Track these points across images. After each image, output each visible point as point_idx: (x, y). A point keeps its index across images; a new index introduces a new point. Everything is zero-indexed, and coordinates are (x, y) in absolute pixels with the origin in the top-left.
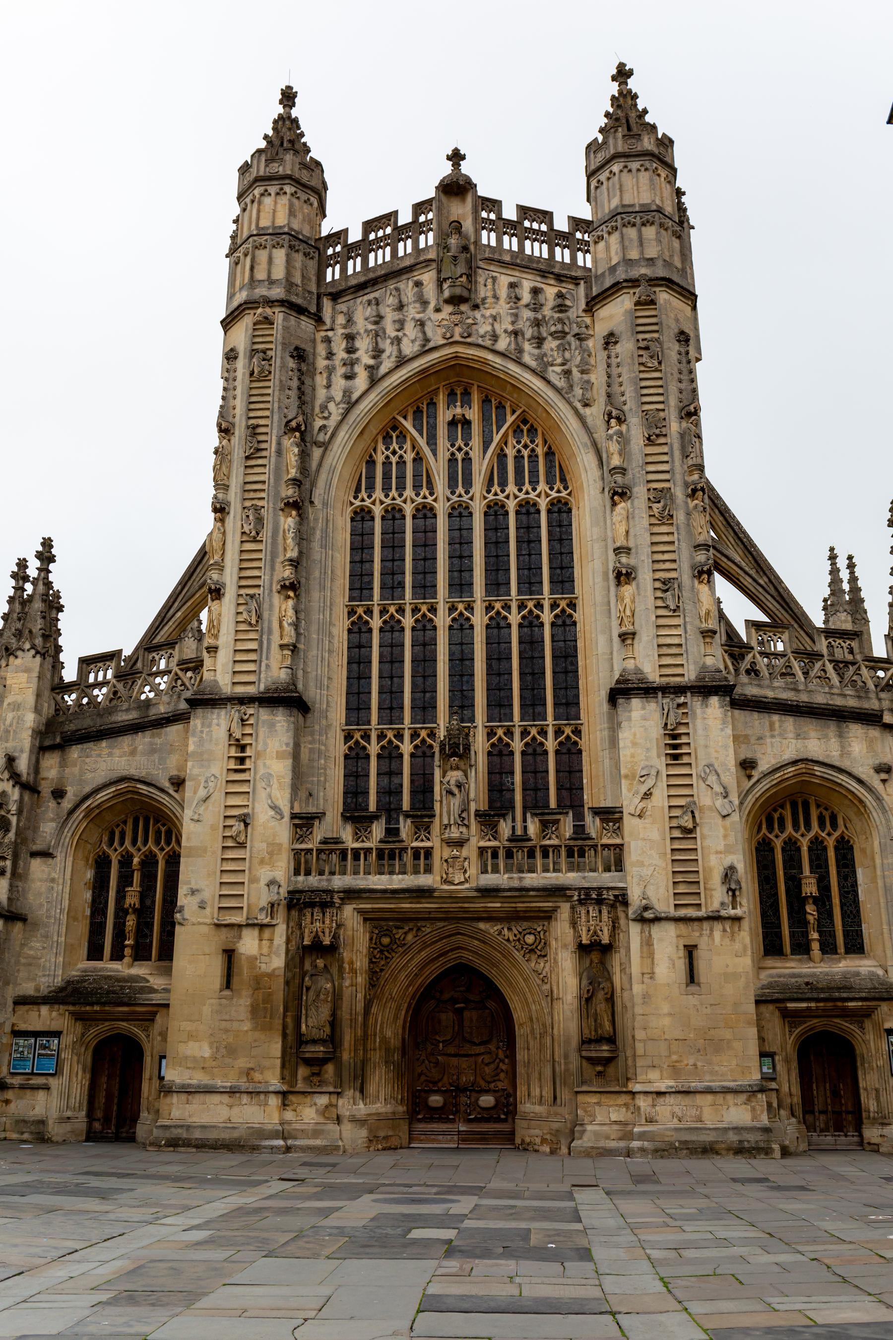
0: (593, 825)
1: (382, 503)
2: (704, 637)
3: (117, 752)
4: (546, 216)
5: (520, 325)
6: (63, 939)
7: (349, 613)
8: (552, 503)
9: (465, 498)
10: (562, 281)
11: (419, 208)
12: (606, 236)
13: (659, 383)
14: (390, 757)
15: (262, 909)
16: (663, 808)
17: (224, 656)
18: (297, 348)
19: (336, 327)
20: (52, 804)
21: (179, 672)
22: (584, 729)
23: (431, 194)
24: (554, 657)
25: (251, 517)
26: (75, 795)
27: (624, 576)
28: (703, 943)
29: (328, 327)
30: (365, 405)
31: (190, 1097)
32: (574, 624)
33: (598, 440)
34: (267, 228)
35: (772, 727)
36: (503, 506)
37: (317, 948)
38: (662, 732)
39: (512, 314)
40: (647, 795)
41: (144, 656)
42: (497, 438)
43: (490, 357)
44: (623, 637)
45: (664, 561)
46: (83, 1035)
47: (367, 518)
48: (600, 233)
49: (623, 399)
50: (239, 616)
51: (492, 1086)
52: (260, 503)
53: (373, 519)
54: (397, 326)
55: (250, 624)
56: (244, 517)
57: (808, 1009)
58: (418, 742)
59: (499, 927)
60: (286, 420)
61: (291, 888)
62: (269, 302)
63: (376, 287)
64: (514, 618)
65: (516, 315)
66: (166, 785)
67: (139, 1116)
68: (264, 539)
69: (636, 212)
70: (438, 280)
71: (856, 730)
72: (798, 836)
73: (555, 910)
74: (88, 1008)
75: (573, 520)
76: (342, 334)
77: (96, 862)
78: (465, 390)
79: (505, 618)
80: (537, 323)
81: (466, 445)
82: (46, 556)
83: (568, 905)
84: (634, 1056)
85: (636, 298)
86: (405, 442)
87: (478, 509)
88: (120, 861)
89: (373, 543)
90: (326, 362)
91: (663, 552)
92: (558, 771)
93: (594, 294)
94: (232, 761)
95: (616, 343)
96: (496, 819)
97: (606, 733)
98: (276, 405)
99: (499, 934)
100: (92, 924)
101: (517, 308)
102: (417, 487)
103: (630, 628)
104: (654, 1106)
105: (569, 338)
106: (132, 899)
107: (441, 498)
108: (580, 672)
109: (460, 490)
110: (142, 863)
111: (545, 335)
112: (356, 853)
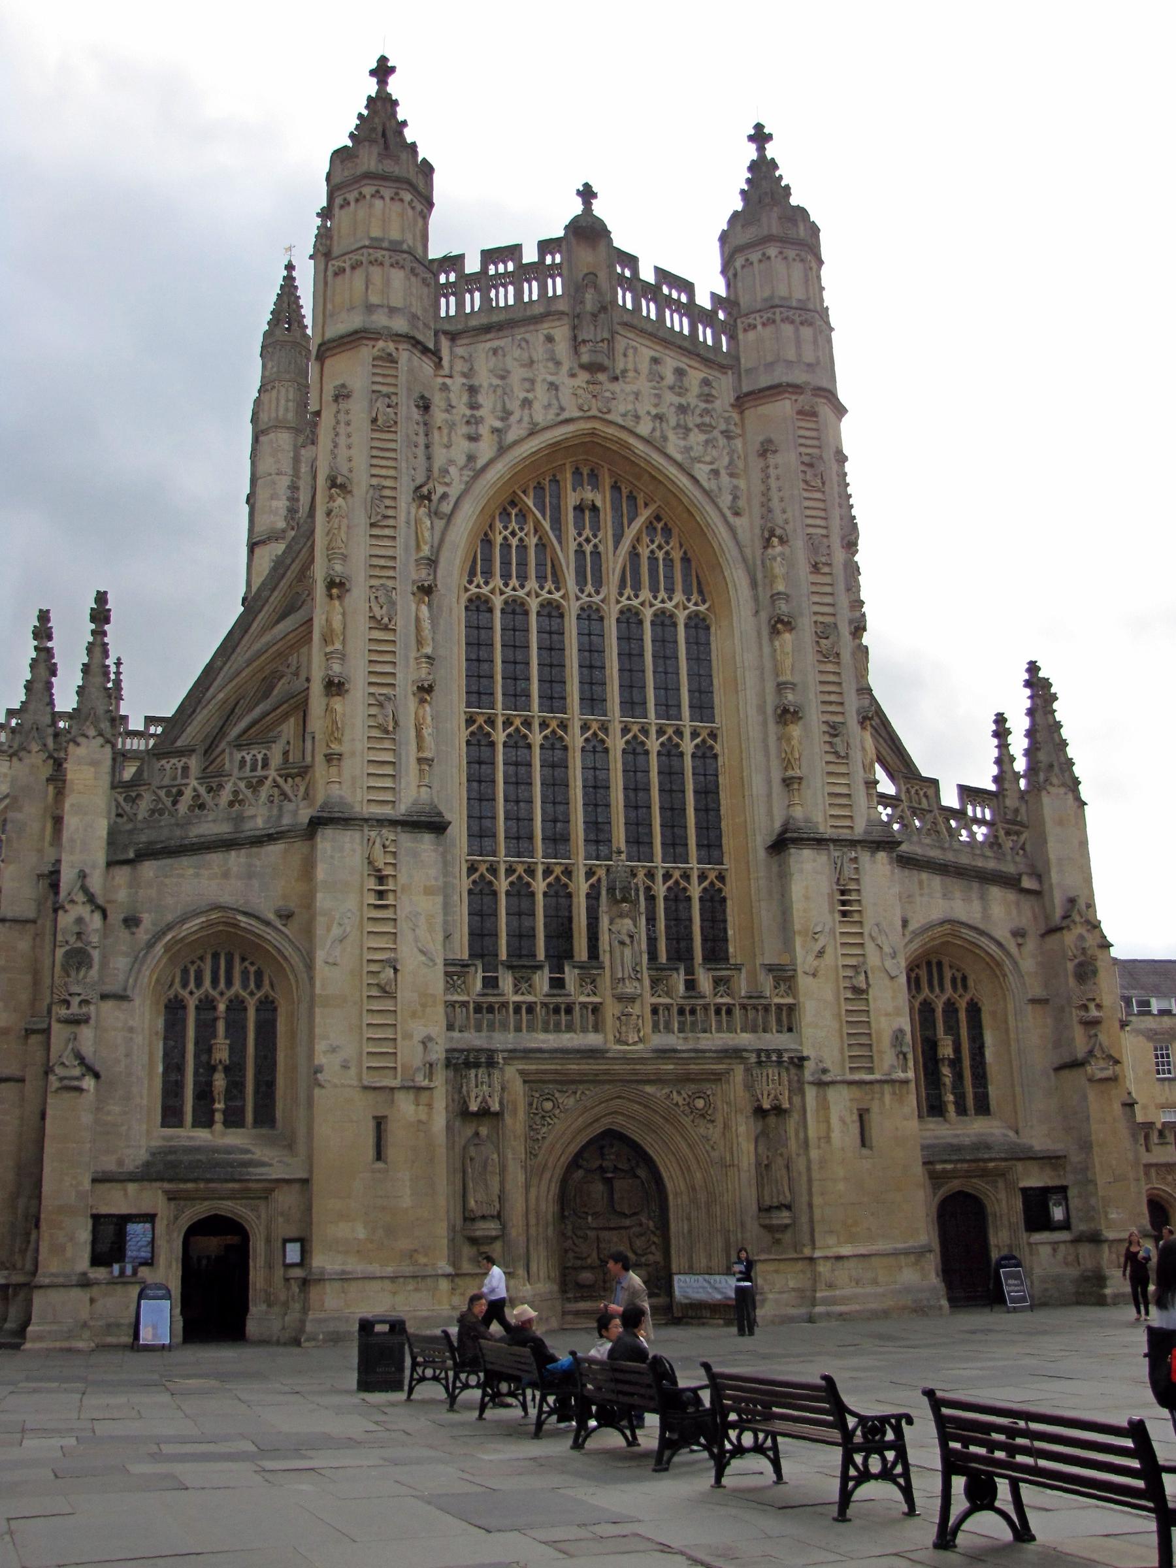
0: (767, 983)
1: (502, 593)
2: (867, 788)
3: (205, 873)
4: (687, 287)
5: (663, 409)
6: (145, 1102)
7: (467, 721)
8: (689, 617)
9: (597, 599)
10: (710, 368)
11: (545, 246)
12: (759, 327)
13: (820, 505)
14: (519, 894)
15: (418, 1069)
16: (837, 966)
17: (354, 767)
18: (422, 397)
19: (454, 374)
20: (124, 934)
21: (279, 779)
22: (731, 878)
23: (561, 233)
24: (696, 792)
25: (382, 600)
26: (154, 924)
27: (787, 715)
28: (875, 1108)
29: (446, 371)
30: (492, 475)
31: (346, 1285)
32: (715, 756)
33: (750, 557)
34: (382, 240)
35: (921, 883)
36: (637, 614)
37: (484, 1113)
38: (835, 887)
39: (656, 395)
40: (821, 954)
41: (231, 754)
42: (630, 533)
43: (632, 440)
44: (787, 782)
45: (831, 703)
46: (176, 1218)
47: (483, 608)
48: (751, 321)
49: (785, 516)
50: (372, 719)
51: (643, 1259)
52: (390, 583)
53: (490, 610)
54: (527, 385)
55: (386, 732)
56: (372, 598)
57: (954, 1170)
58: (551, 879)
59: (667, 1090)
60: (412, 486)
61: (448, 1047)
62: (398, 337)
63: (501, 334)
64: (653, 745)
65: (658, 396)
66: (271, 916)
67: (246, 1310)
68: (398, 629)
69: (796, 309)
70: (575, 338)
71: (995, 892)
72: (933, 997)
73: (728, 1072)
74: (190, 1186)
75: (712, 638)
76: (464, 384)
77: (166, 1007)
78: (592, 470)
79: (643, 743)
80: (682, 409)
81: (595, 536)
82: (100, 615)
83: (742, 1067)
84: (811, 1221)
85: (798, 406)
86: (525, 522)
87: (612, 613)
88: (197, 1008)
89: (492, 638)
90: (445, 416)
91: (829, 693)
92: (702, 920)
93: (745, 389)
94: (373, 894)
95: (775, 452)
96: (669, 973)
97: (762, 882)
98: (404, 465)
99: (668, 1096)
100: (165, 1082)
101: (660, 389)
102: (541, 578)
103: (797, 773)
104: (833, 1270)
105: (716, 433)
106: (221, 1053)
107: (572, 597)
108: (722, 812)
109: (589, 588)
110: (228, 1008)
111: (691, 425)
112: (517, 1008)
